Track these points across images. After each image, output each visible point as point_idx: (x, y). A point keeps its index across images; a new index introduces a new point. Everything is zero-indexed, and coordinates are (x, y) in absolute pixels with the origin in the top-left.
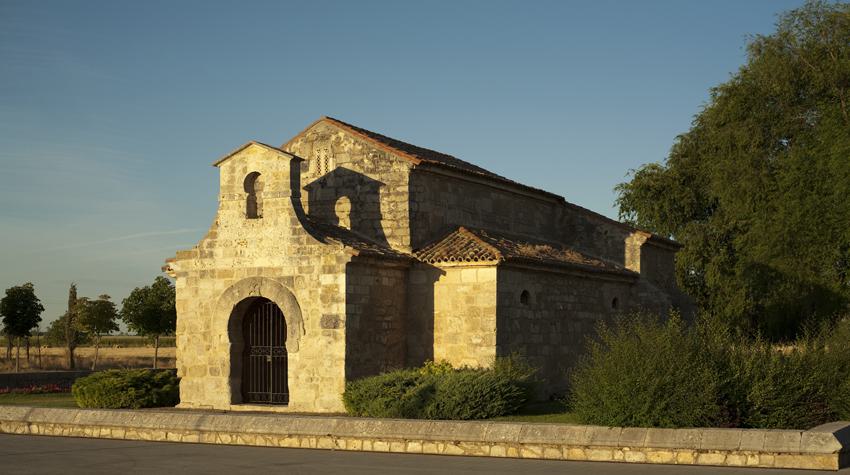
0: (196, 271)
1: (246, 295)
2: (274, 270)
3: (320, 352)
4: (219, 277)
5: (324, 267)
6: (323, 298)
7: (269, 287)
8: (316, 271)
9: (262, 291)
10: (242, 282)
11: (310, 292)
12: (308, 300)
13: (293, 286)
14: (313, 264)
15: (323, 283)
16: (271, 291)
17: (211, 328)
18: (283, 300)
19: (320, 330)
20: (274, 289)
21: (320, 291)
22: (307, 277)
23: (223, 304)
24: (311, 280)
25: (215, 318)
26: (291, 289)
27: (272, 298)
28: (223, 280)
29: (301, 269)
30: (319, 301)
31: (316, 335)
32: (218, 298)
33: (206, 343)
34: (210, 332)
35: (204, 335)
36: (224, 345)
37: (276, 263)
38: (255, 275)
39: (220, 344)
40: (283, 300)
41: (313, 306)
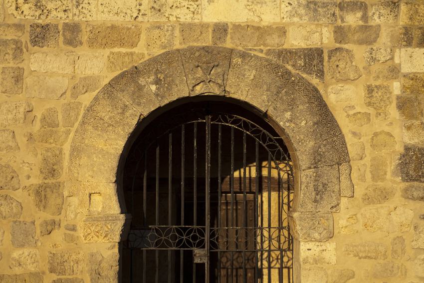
0: (19, 27)
1: (181, 90)
2: (261, 32)
3: (400, 239)
4: (92, 43)
5: (407, 31)
6: (403, 105)
7: (251, 74)
8: (384, 39)
9: (232, 79)
10: (168, 58)
11: (370, 90)
12: (358, 109)
13: (321, 74)
14: (376, 21)
15: (406, 69)
16: (256, 84)
17: (63, 177)
18: (292, 105)
19: (394, 182)
20: (267, 78)
21: (396, 87)
22: (360, 53)
23: (105, 112)
24: (374, 60)
25: (76, 151)
26: (315, 81)
27: (259, 100)
28: (107, 52)
29: (341, 33)
30: (393, 112)
31: (384, 195)
32: (86, 99)
33: (47, 216)
34: (58, 186)
35: (41, 195)
36: (107, 219)
37: (269, 16)
38: (207, 40)
39: (92, 219)
40: (292, 105)
41: (379, 125)
